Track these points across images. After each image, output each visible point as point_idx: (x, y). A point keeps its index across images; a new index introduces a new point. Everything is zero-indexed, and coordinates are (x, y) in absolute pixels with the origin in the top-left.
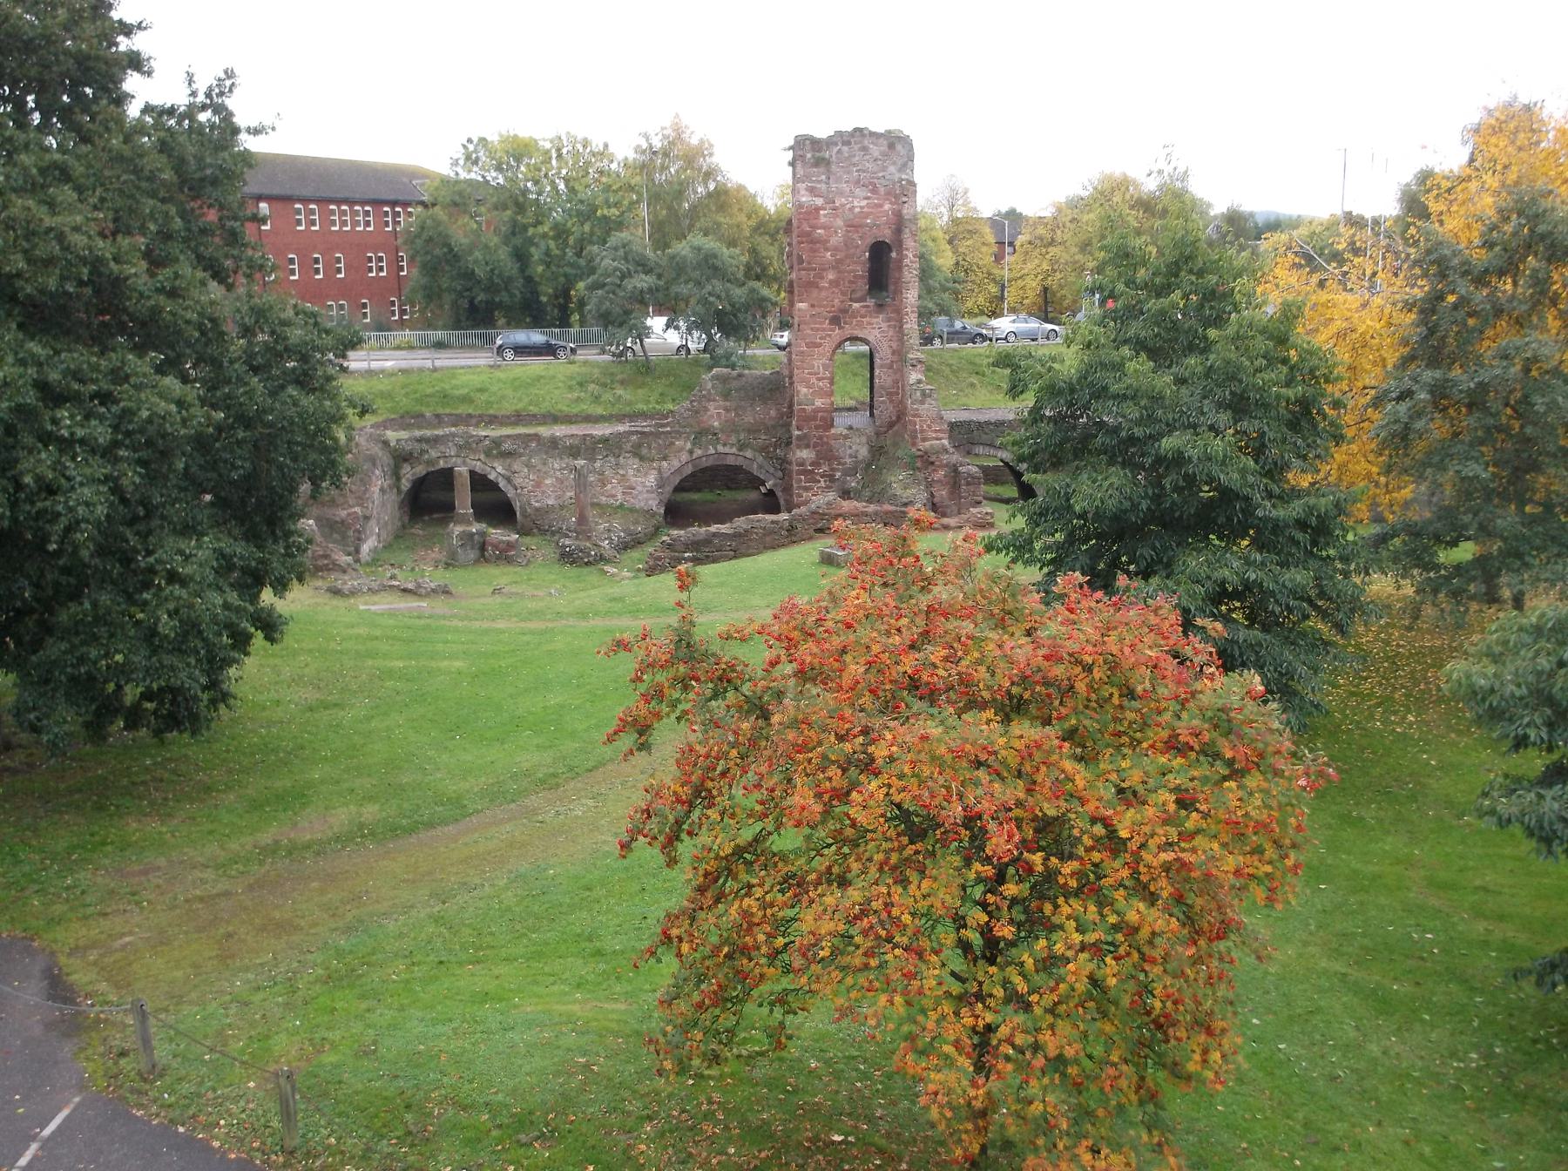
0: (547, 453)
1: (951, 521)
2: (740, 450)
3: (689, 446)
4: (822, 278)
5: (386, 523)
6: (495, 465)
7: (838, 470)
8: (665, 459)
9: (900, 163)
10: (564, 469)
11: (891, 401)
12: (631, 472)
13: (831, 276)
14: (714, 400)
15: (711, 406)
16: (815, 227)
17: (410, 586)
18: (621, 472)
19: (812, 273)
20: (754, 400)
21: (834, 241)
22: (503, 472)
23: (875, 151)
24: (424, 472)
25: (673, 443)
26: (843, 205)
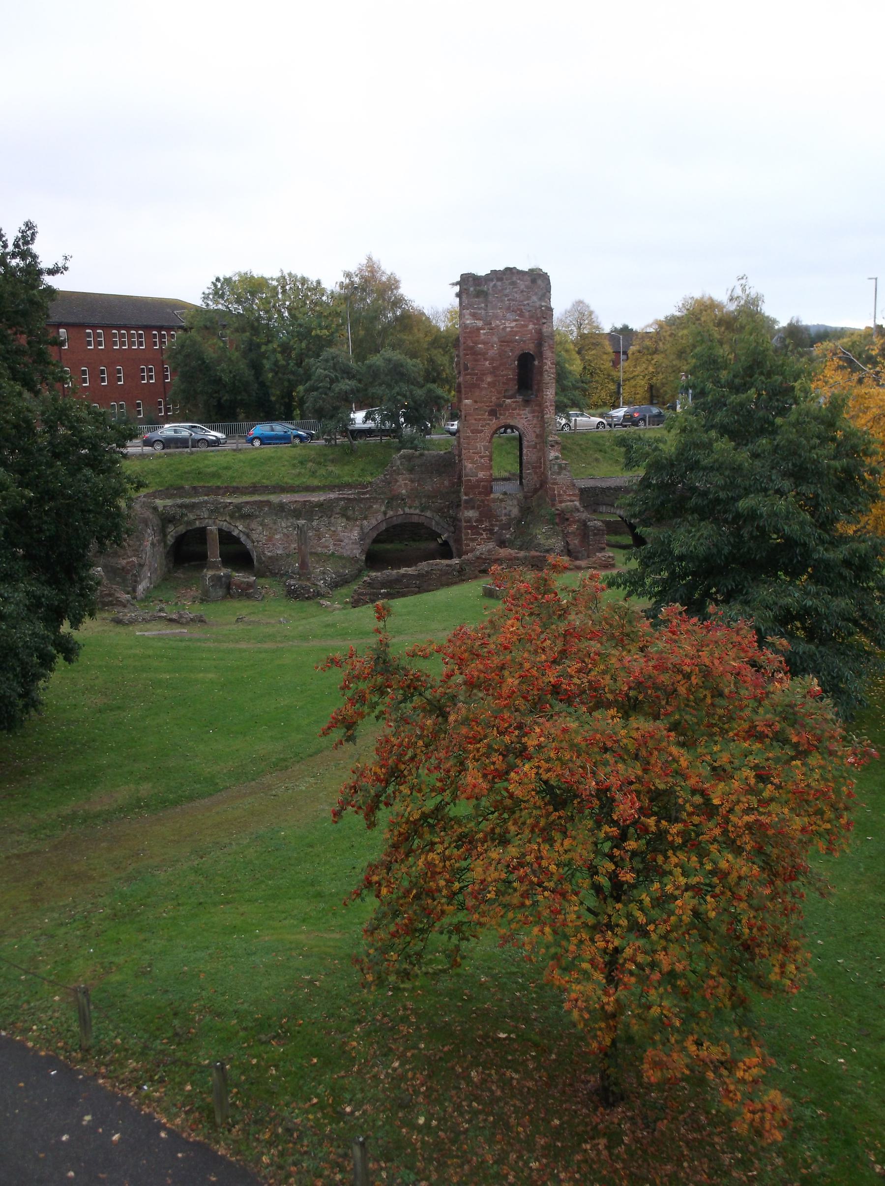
0: (276, 515)
1: (582, 563)
2: (422, 511)
3: (383, 508)
4: (483, 381)
5: (156, 569)
6: (237, 524)
7: (496, 525)
8: (365, 518)
9: (540, 293)
10: (289, 527)
11: (536, 473)
12: (340, 528)
13: (489, 379)
14: (402, 474)
15: (400, 478)
16: (476, 343)
17: (174, 617)
18: (332, 529)
19: (475, 377)
20: (432, 473)
21: (491, 353)
23: (522, 285)
24: (184, 531)
25: (372, 507)
26: (498, 326)
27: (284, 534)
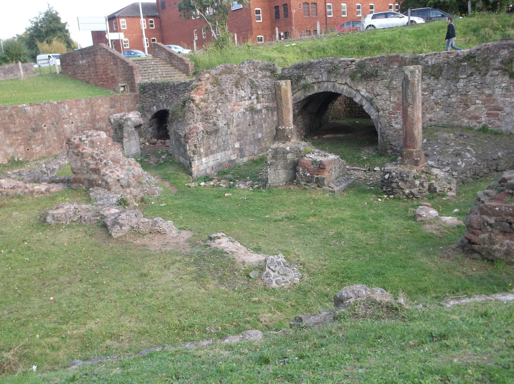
6: (360, 88)
12: (498, 91)
18: (487, 92)
22: (367, 95)
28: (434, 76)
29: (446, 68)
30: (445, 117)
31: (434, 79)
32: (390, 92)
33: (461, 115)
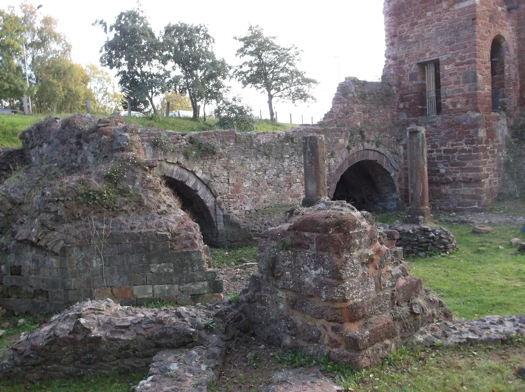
0: (243, 152)
6: (196, 168)
8: (332, 155)
10: (259, 171)
14: (357, 103)
25: (337, 141)
27: (254, 181)
28: (266, 155)
29: (274, 147)
30: (276, 197)
31: (266, 159)
32: (228, 173)
33: (287, 194)
